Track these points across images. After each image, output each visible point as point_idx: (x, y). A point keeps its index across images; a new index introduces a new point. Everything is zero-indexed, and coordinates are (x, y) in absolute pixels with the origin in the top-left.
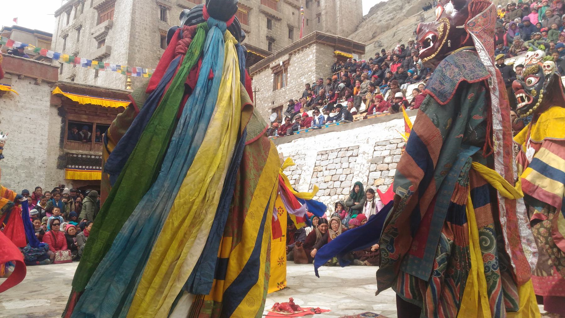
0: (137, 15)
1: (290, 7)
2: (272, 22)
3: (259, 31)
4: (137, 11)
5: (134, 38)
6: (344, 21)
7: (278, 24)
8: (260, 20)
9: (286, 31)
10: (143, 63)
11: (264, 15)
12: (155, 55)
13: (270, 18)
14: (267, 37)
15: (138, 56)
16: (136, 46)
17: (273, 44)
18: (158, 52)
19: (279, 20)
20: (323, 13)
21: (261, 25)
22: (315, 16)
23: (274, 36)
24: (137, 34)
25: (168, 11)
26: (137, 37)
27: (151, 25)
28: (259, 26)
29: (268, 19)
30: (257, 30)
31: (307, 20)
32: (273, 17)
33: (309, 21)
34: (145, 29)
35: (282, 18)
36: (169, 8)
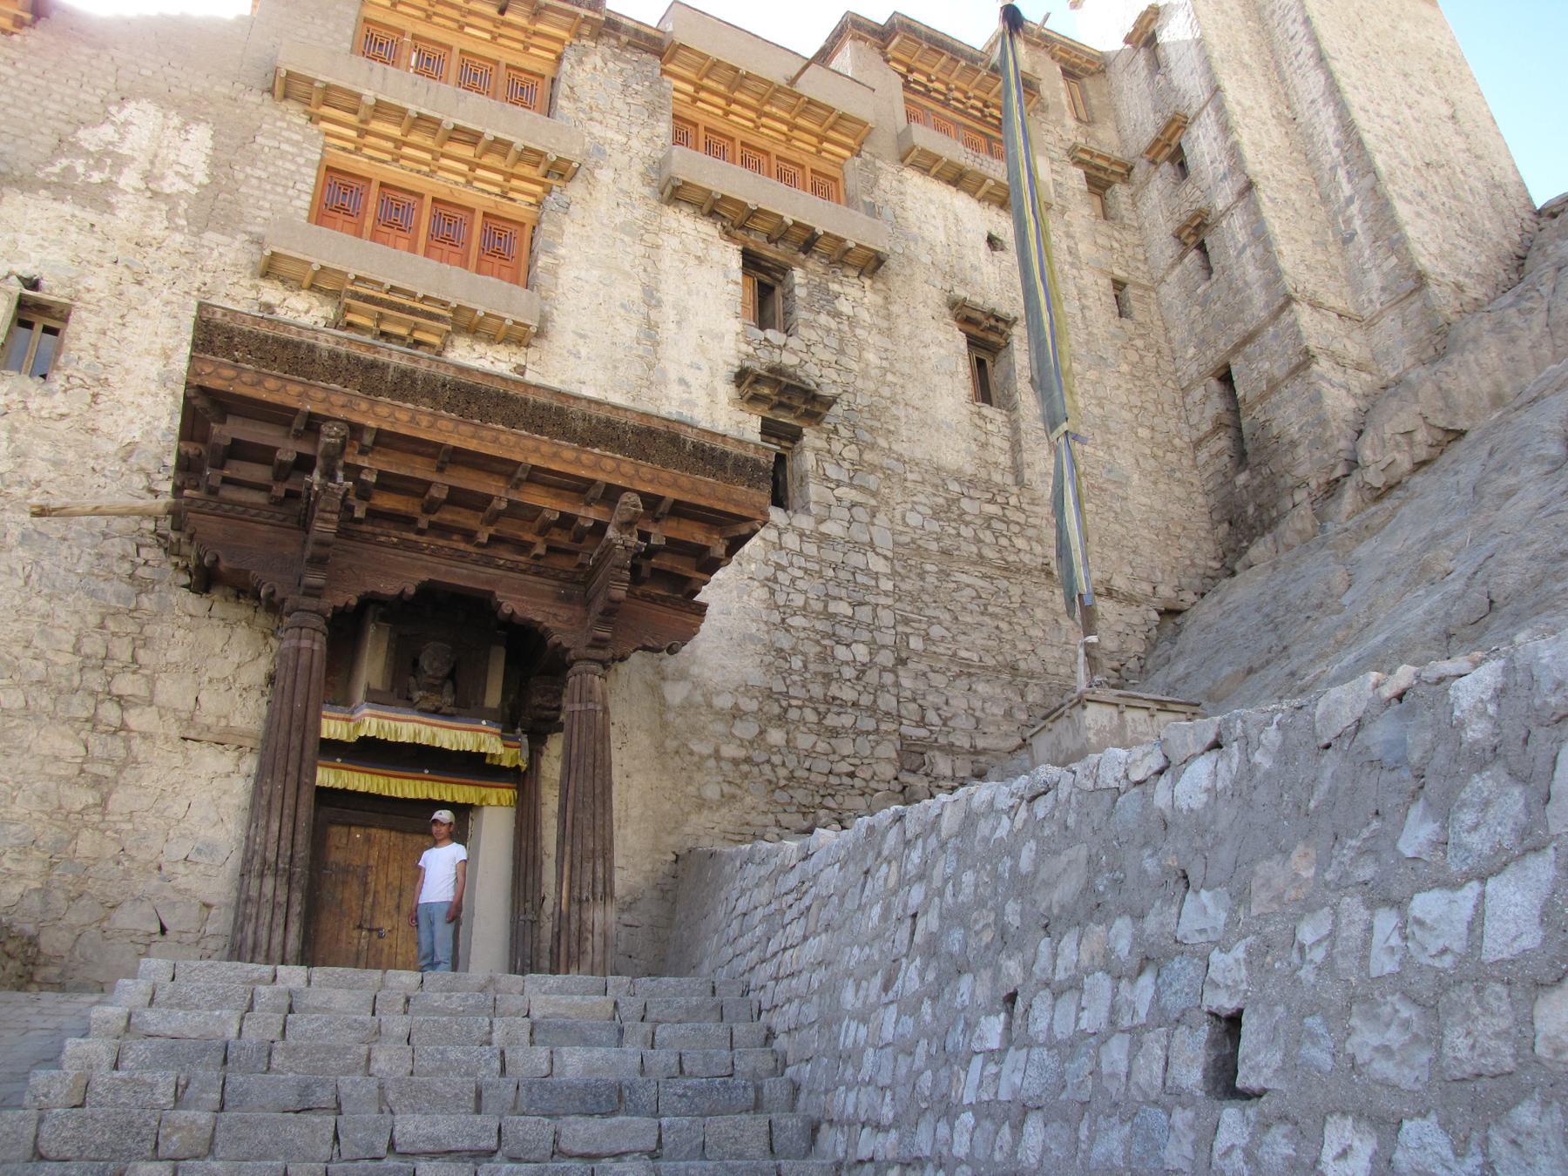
1: (961, 202)
2: (798, 275)
3: (650, 330)
6: (1403, 211)
7: (854, 295)
8: (668, 261)
9: (948, 349)
11: (708, 229)
13: (770, 252)
14: (742, 377)
17: (811, 438)
19: (872, 264)
21: (670, 290)
22: (1171, 250)
23: (821, 375)
28: (651, 297)
29: (751, 261)
30: (629, 331)
31: (1119, 285)
32: (808, 241)
33: (1131, 292)
35: (880, 244)
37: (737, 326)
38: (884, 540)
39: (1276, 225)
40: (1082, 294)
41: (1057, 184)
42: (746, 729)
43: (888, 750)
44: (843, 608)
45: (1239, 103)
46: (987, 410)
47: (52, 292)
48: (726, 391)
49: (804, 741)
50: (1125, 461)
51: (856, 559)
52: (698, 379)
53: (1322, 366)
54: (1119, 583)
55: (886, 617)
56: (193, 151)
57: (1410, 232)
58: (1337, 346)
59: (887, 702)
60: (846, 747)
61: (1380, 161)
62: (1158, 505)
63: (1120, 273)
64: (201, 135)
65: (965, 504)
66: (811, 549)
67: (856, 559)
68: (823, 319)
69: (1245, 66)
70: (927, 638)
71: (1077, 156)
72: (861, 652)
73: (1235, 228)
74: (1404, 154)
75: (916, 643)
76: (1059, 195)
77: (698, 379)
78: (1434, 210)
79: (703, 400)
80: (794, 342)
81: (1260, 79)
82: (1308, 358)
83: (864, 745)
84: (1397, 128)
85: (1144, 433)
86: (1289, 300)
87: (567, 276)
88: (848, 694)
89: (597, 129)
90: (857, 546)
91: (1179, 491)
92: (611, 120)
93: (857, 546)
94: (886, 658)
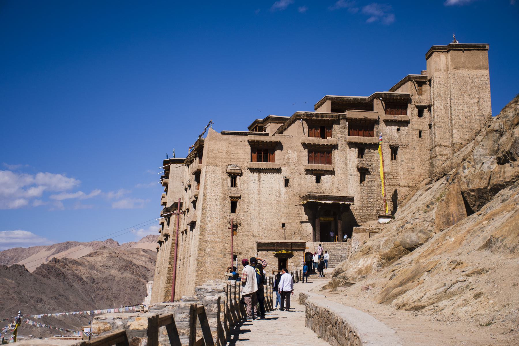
0: (208, 190)
3: (346, 165)
4: (208, 186)
5: (206, 211)
6: (455, 131)
8: (348, 152)
10: (214, 231)
12: (226, 221)
14: (357, 168)
15: (208, 226)
16: (208, 218)
18: (228, 217)
20: (433, 124)
21: (348, 157)
24: (208, 206)
25: (238, 177)
26: (207, 209)
27: (221, 195)
28: (346, 159)
30: (343, 165)
31: (420, 132)
34: (216, 200)
36: (241, 174)
37: (357, 159)
38: (376, 185)
39: (437, 132)
40: (412, 136)
41: (412, 113)
42: (358, 211)
43: (375, 211)
44: (370, 195)
45: (437, 107)
46: (394, 161)
47: (288, 178)
48: (356, 169)
49: (364, 211)
50: (415, 165)
51: (372, 188)
52: (352, 169)
53: (438, 157)
54: (410, 185)
55: (375, 195)
56: (295, 156)
57: (454, 136)
58: (442, 153)
59: (375, 205)
60: (369, 211)
61: (453, 122)
62: (420, 171)
63: (421, 129)
64: (296, 153)
65: (388, 177)
66: (366, 188)
67: (372, 188)
68: (369, 154)
69: (441, 96)
70: (381, 197)
71: (417, 107)
72: (372, 200)
73: (433, 128)
74: (461, 117)
75: (379, 198)
76: (412, 116)
77: (352, 169)
78: (463, 128)
79: (352, 171)
80: (364, 159)
81: (443, 98)
82: (436, 156)
83: (372, 211)
84: (461, 111)
85: (419, 159)
86: (436, 146)
87: (336, 160)
88: (370, 205)
89: (338, 135)
90: (371, 186)
91: (424, 168)
92: (340, 133)
93: (371, 186)
94: (375, 200)
